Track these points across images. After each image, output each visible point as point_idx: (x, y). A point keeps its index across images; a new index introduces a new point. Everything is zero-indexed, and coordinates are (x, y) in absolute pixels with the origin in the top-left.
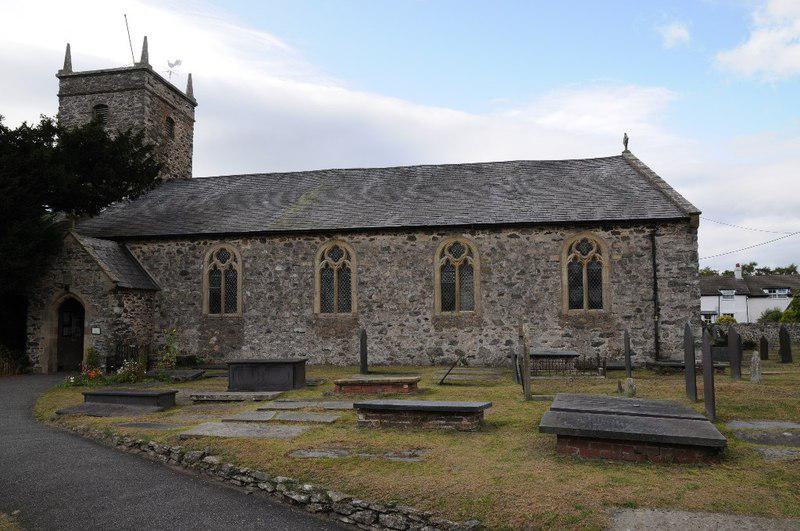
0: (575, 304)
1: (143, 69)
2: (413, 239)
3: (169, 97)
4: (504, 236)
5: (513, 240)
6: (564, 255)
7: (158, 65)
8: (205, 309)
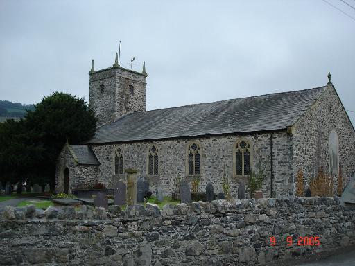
0: (239, 172)
1: (116, 67)
2: (178, 142)
3: (131, 77)
4: (212, 139)
5: (214, 142)
6: (234, 149)
7: (124, 64)
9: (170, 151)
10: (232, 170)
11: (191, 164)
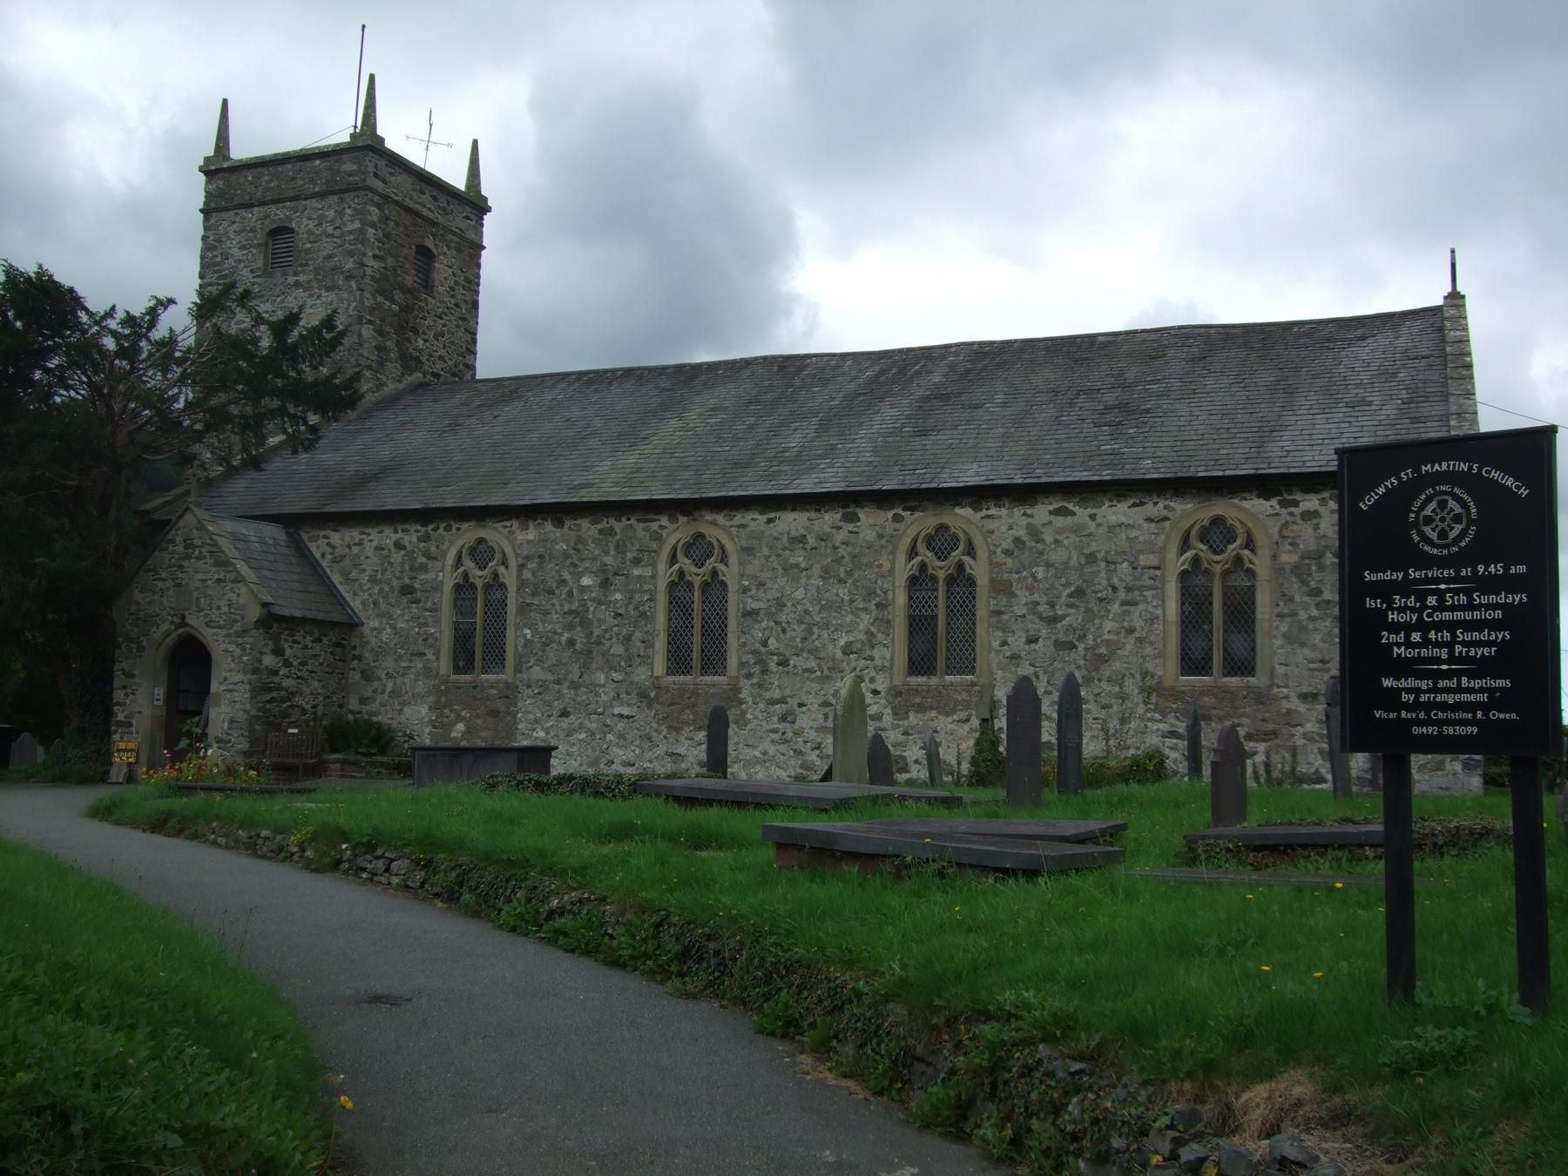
0: (1193, 663)
1: (366, 141)
2: (853, 518)
3: (424, 203)
4: (1041, 512)
5: (1060, 522)
6: (1172, 553)
7: (399, 135)
8: (445, 666)
9: (798, 558)
10: (1161, 655)
11: (919, 624)
